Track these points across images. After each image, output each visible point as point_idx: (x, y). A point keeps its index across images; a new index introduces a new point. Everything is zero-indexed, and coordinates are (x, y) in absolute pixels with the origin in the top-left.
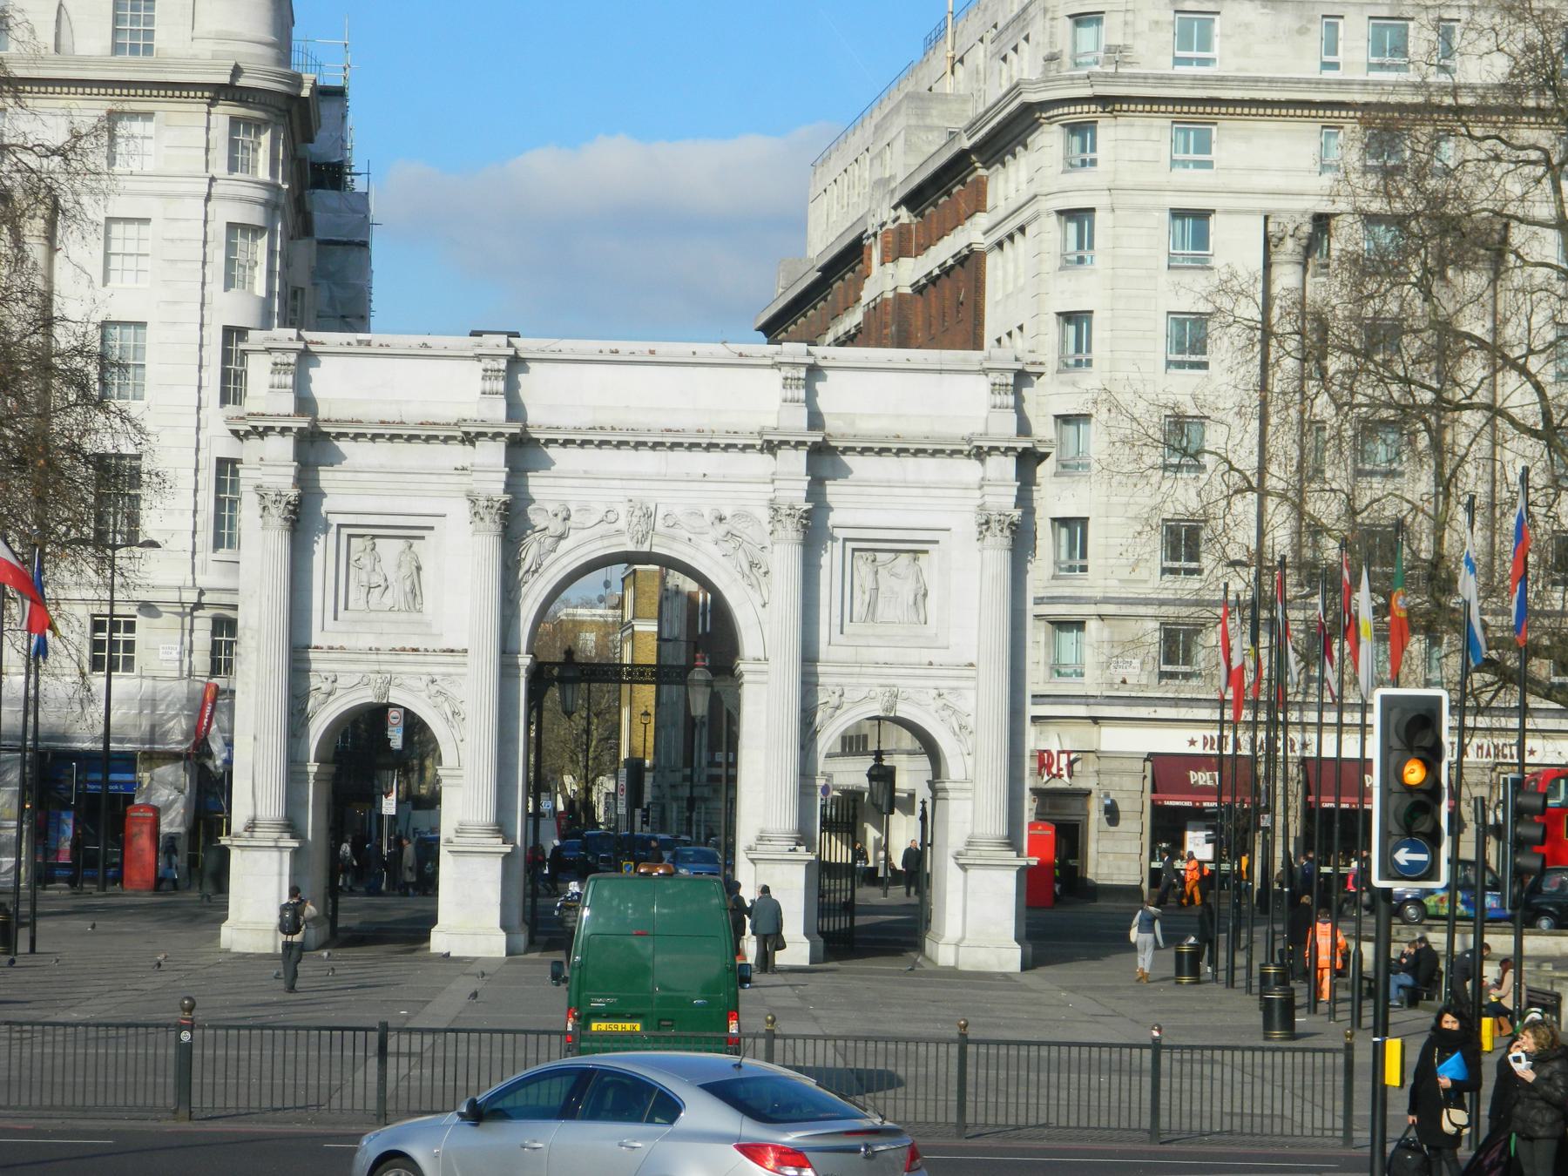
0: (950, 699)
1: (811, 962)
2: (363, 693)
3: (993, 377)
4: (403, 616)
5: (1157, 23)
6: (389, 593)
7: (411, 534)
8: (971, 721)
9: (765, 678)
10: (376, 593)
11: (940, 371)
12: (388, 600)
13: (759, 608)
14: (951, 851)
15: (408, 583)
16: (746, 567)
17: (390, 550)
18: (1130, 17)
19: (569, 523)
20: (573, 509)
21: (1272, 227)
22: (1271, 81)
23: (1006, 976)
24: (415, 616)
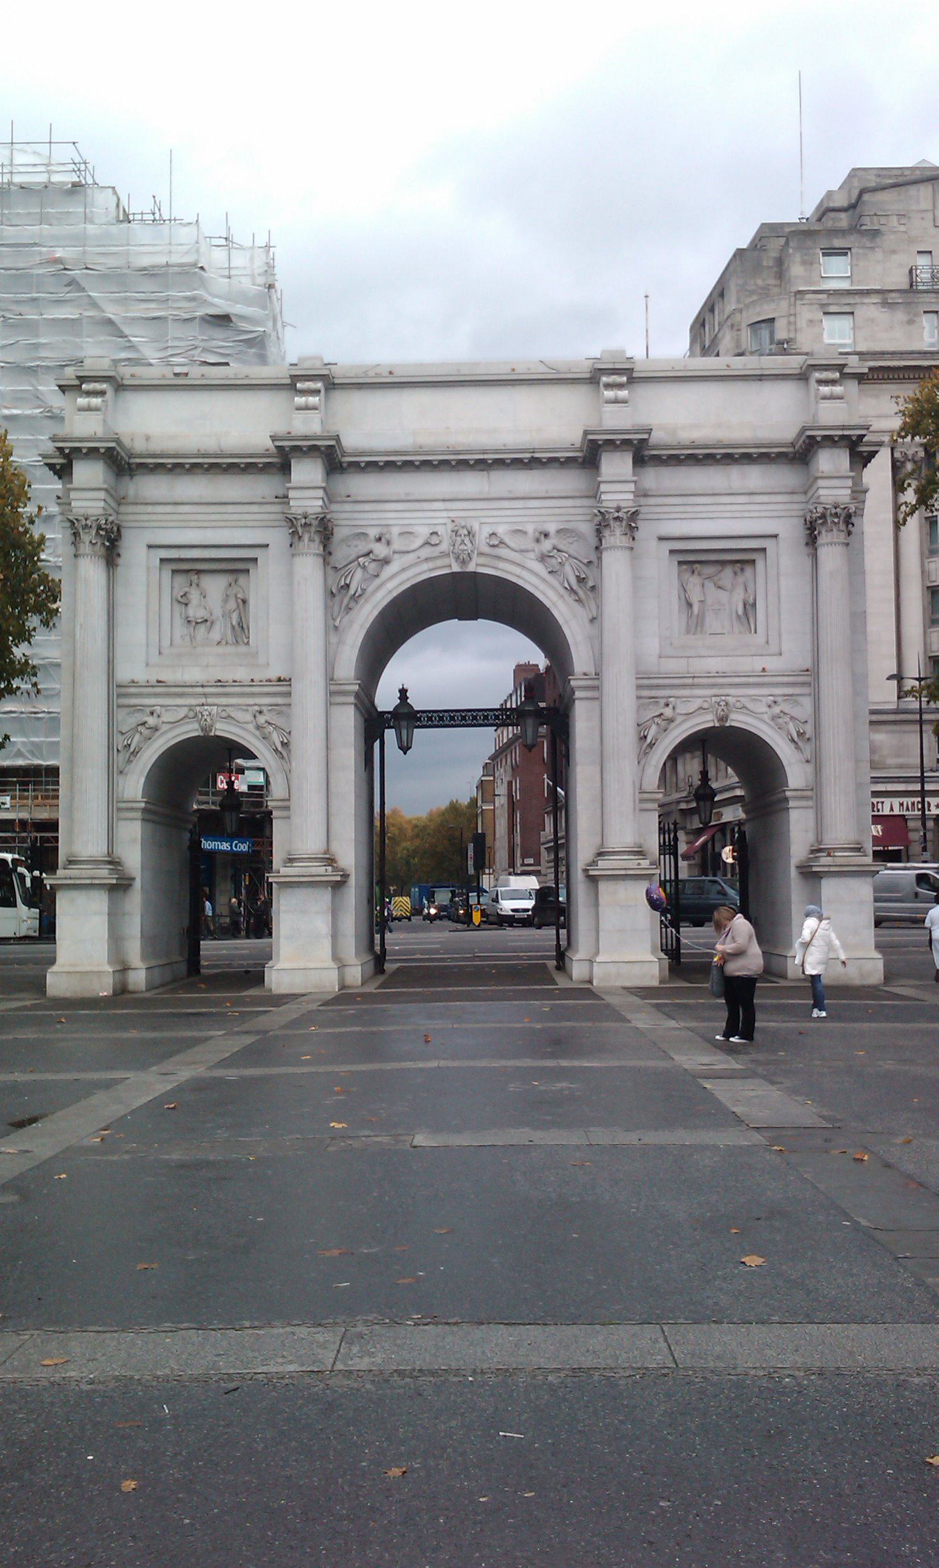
0: (786, 707)
1: (661, 982)
2: (190, 727)
3: (817, 375)
4: (230, 649)
5: (811, 321)
6: (217, 627)
7: (237, 567)
8: (809, 729)
9: (594, 694)
10: (202, 629)
11: (761, 378)
12: (216, 634)
13: (587, 624)
14: (794, 861)
15: (235, 616)
16: (573, 581)
17: (215, 586)
18: (792, 319)
19: (396, 546)
20: (395, 531)
21: (897, 455)
22: (893, 353)
23: (875, 987)
24: (242, 649)
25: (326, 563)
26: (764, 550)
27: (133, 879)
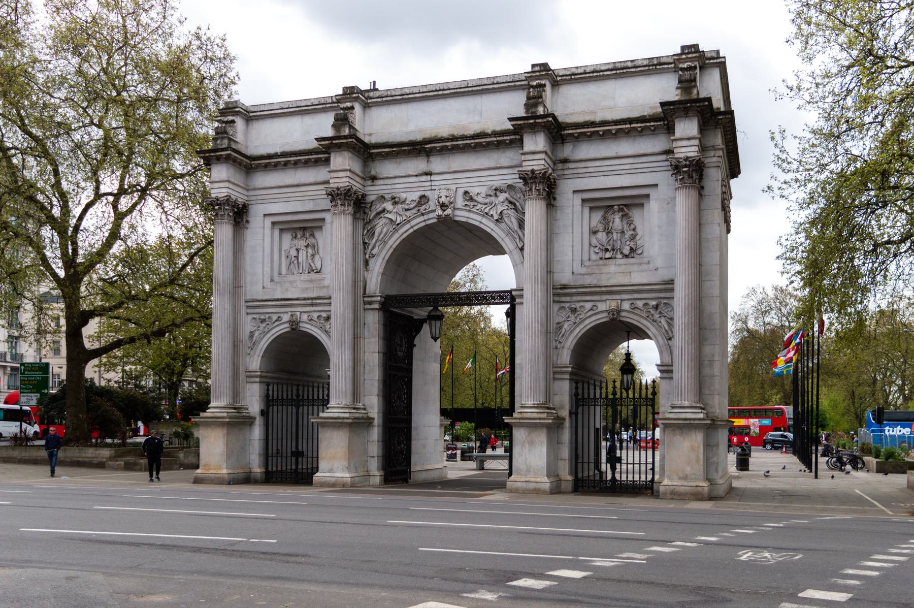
25: (355, 218)
26: (648, 196)
27: (374, 419)
